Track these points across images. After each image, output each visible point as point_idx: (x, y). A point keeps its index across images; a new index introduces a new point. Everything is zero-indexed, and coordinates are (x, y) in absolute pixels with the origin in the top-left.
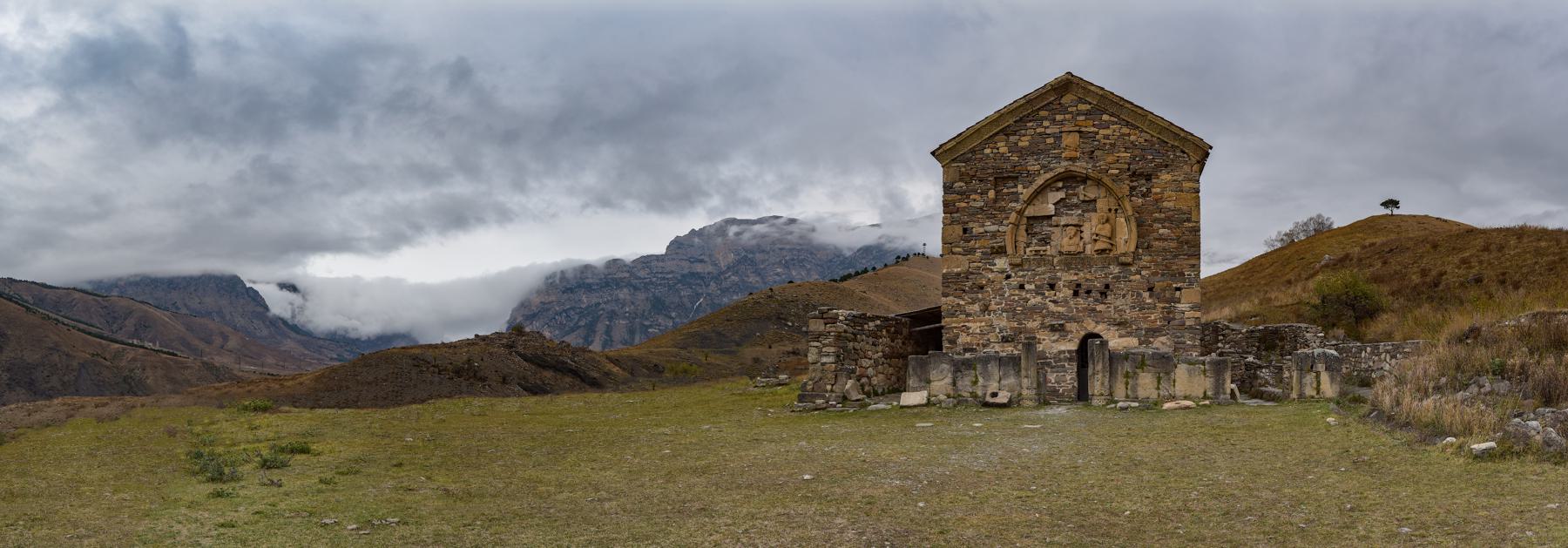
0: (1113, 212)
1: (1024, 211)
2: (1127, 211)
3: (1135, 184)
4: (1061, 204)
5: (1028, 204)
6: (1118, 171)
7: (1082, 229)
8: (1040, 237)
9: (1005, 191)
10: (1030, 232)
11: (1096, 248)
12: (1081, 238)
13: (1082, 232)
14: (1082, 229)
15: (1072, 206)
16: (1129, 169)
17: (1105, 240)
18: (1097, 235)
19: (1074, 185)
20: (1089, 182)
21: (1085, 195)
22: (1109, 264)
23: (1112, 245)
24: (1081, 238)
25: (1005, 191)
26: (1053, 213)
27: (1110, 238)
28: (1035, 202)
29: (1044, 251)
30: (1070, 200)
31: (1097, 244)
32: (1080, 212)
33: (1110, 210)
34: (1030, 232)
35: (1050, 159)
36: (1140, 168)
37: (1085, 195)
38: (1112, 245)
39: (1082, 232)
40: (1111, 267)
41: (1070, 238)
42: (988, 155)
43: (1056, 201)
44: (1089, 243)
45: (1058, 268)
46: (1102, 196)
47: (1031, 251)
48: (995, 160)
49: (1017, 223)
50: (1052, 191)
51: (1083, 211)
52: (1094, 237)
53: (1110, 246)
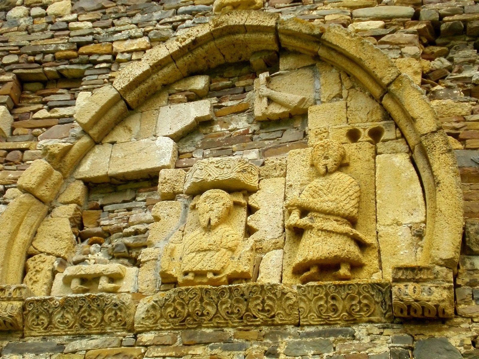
0: (364, 136)
1: (78, 163)
2: (412, 120)
3: (440, 63)
4: (198, 139)
5: (97, 142)
6: (381, 23)
7: (253, 200)
8: (117, 241)
9: (43, 113)
10: (89, 228)
11: (299, 259)
12: (249, 231)
13: (251, 210)
14: (253, 200)
15: (230, 140)
16: (416, 17)
17: (332, 224)
18: (304, 212)
19: (242, 83)
20: (284, 64)
21: (270, 100)
22: (355, 322)
23: (361, 245)
24: (249, 231)
25: (43, 113)
26: (167, 160)
27: (352, 222)
28: (120, 135)
29: (114, 278)
30: (225, 124)
31: (308, 239)
32: (253, 155)
33: (353, 135)
34: (89, 228)
35: (178, 18)
36: (453, 13)
37: (270, 100)
38: (361, 245)
39: (251, 210)
40: (360, 331)
41: (209, 228)
42: (15, 22)
43: (179, 126)
44: (276, 247)
45: (147, 337)
46: (325, 94)
47: (67, 281)
48: (29, 31)
49: (43, 192)
50: (170, 101)
51: (264, 153)
52: (295, 219)
53: (353, 249)
